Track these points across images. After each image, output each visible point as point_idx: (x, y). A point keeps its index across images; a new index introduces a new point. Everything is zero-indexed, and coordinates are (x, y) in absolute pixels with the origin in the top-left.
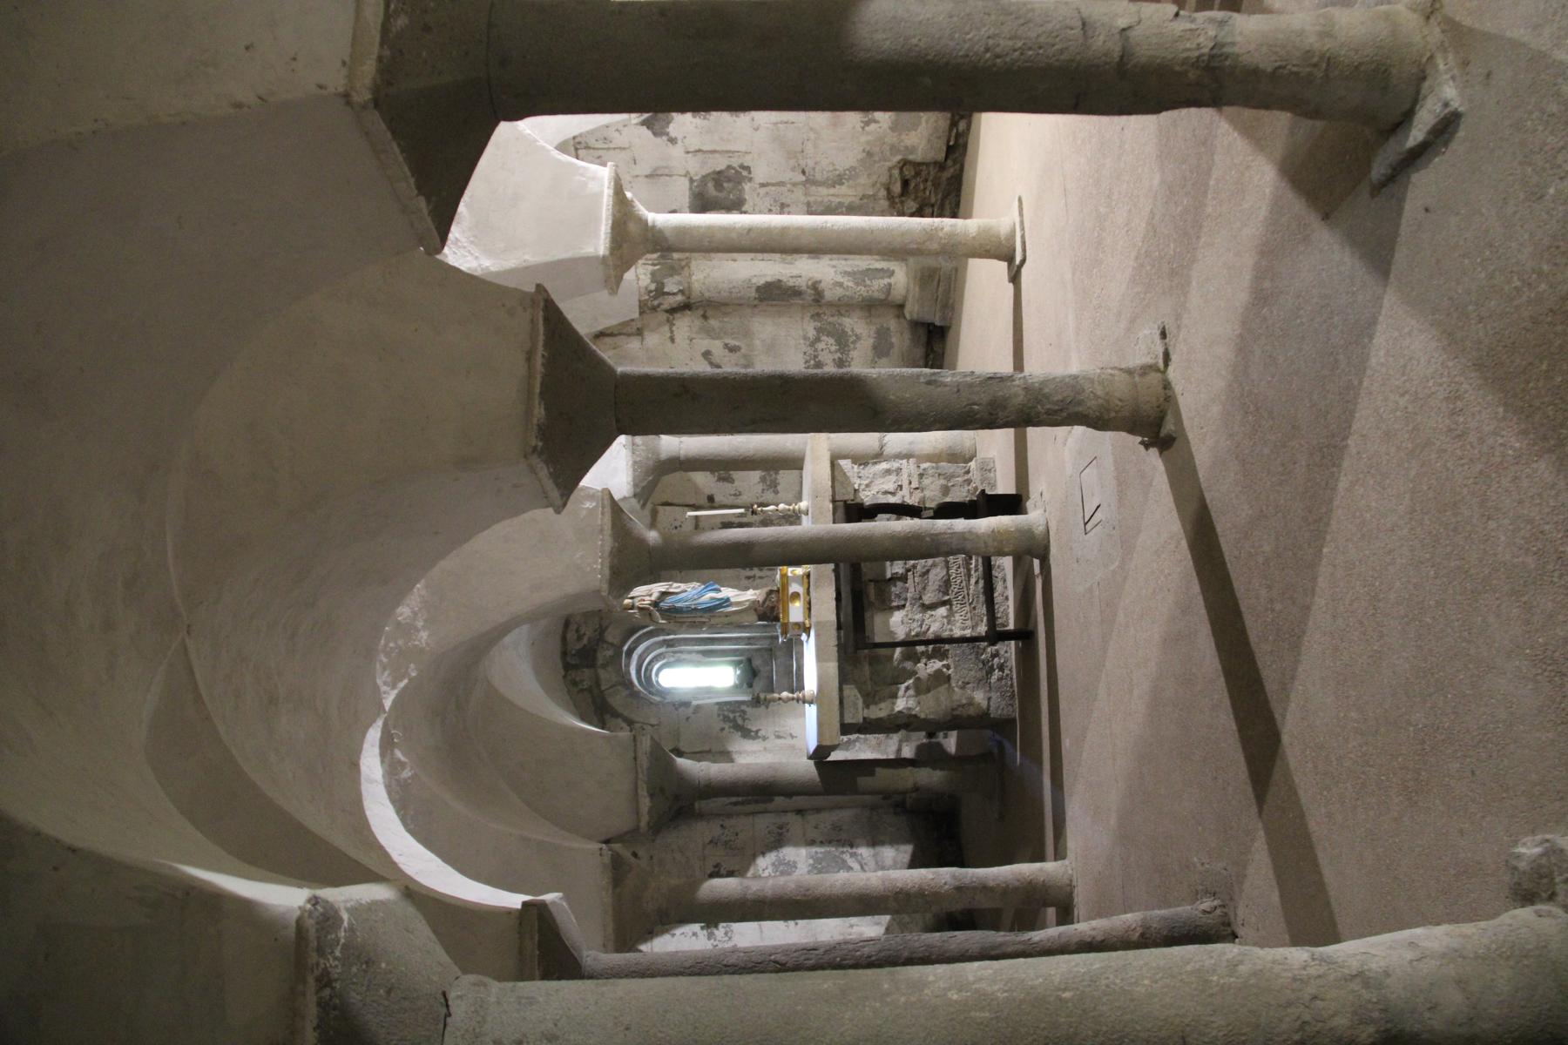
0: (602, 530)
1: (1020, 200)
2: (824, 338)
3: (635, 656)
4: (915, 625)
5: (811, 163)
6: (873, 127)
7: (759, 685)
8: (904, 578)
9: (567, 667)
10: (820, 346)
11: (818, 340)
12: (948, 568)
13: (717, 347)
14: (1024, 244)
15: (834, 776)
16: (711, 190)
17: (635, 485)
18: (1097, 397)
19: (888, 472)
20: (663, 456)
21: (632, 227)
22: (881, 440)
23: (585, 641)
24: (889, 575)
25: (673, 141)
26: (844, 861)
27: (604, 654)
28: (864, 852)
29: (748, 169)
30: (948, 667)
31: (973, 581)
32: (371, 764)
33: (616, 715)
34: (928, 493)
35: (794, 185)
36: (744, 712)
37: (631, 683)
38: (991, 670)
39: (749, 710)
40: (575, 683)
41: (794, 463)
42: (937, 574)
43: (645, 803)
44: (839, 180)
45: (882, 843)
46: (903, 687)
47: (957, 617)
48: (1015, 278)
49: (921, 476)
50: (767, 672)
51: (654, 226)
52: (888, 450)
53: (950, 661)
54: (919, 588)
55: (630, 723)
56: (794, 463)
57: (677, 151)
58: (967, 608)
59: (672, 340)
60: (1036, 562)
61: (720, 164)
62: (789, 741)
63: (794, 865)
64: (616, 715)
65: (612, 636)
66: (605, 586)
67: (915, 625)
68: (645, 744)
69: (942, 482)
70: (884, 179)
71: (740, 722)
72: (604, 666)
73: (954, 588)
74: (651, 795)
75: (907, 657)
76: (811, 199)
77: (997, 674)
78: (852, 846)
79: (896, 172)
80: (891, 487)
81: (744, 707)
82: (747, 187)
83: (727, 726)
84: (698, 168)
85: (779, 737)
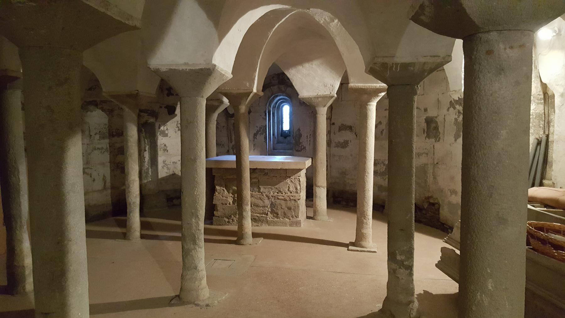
0: (238, 89)
1: (375, 252)
3: (278, 98)
5: (440, 166)
6: (449, 193)
7: (281, 139)
8: (259, 192)
10: (382, 165)
16: (433, 125)
17: (303, 99)
19: (296, 189)
20: (317, 108)
21: (365, 97)
25: (448, 110)
27: (283, 87)
29: (439, 141)
30: (229, 204)
31: (258, 215)
32: (287, 7)
35: (434, 159)
40: (273, 77)
44: (435, 178)
48: (346, 245)
49: (295, 200)
51: (367, 105)
57: (445, 111)
60: (235, 239)
61: (441, 130)
69: (292, 208)
70: (435, 197)
75: (234, 190)
76: (429, 166)
77: (227, 220)
79: (436, 201)
80: (291, 189)
82: (433, 140)
83: (258, 128)
84: (440, 120)
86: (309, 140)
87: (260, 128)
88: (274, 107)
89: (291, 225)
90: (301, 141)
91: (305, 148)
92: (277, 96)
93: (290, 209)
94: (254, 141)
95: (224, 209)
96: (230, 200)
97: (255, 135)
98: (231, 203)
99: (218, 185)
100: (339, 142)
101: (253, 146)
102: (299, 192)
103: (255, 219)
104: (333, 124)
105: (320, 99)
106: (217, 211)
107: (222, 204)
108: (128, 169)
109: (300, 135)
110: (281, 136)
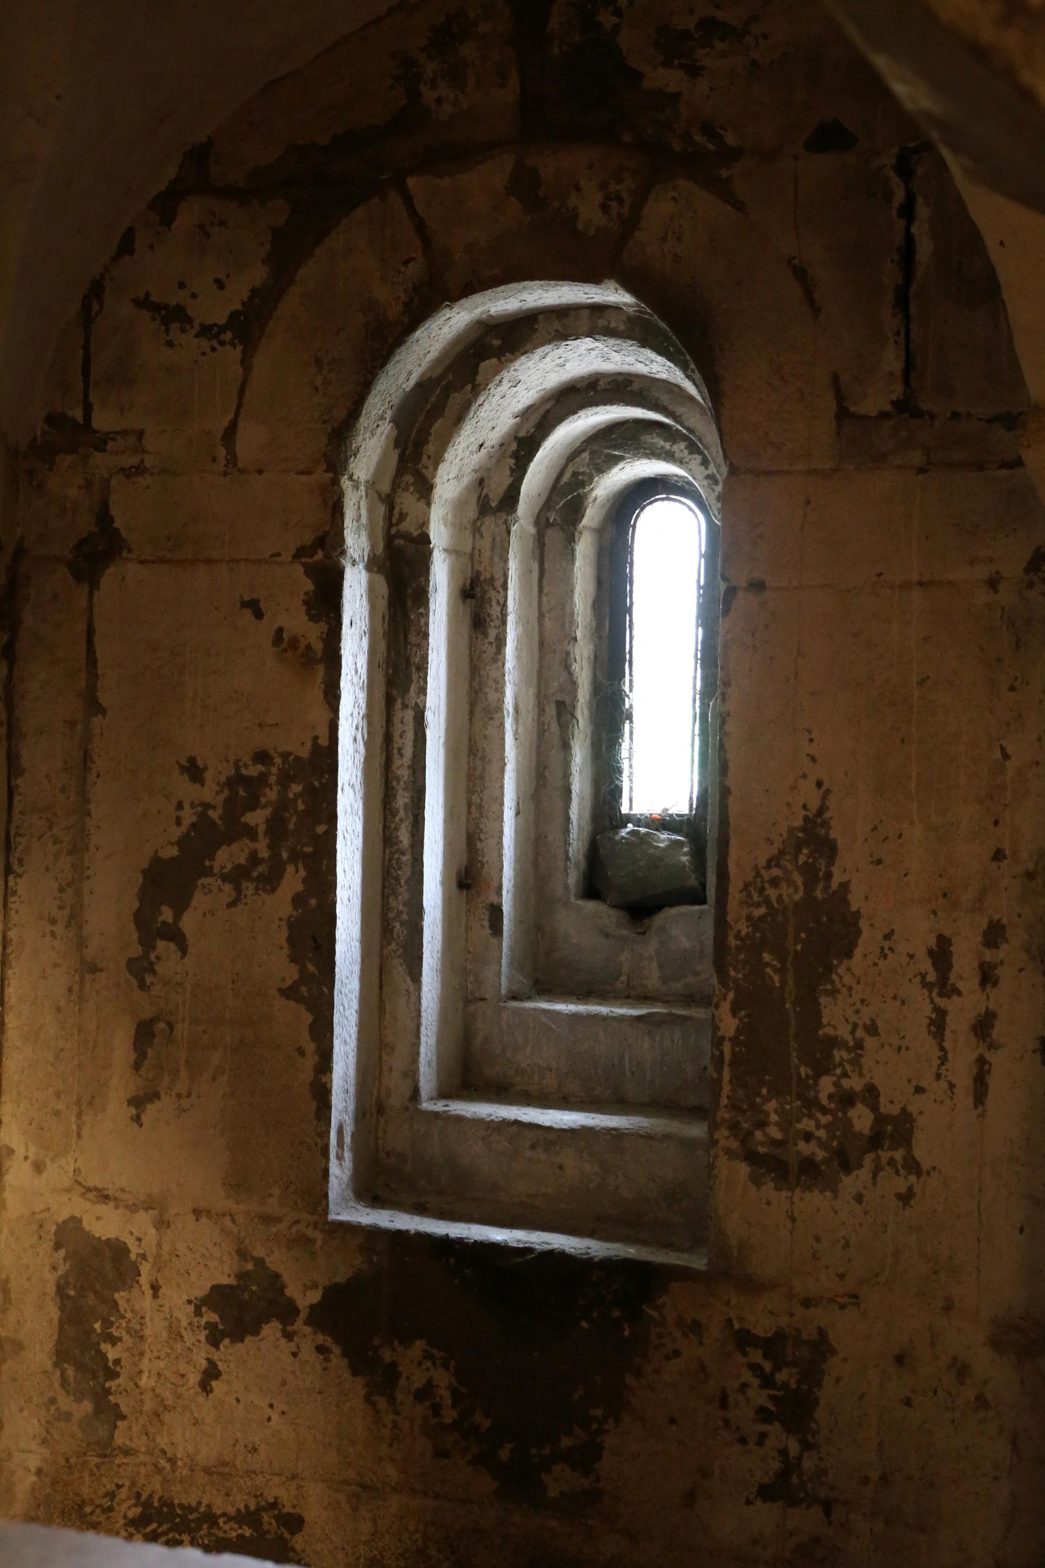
7: (585, 927)
23: (667, 78)
33: (287, 254)
36: (270, 882)
55: (246, 327)
62: (120, 1085)
64: (287, 254)
65: (676, 216)
71: (227, 857)
72: (525, 185)
81: (293, 880)
83: (209, 792)
85: (144, 1035)
86: (962, 1012)
87: (243, 790)
88: (492, 501)
90: (836, 1016)
91: (895, 1131)
92: (515, 336)
94: (141, 969)
97: (166, 885)
101: (122, 1050)
109: (829, 932)
110: (593, 887)
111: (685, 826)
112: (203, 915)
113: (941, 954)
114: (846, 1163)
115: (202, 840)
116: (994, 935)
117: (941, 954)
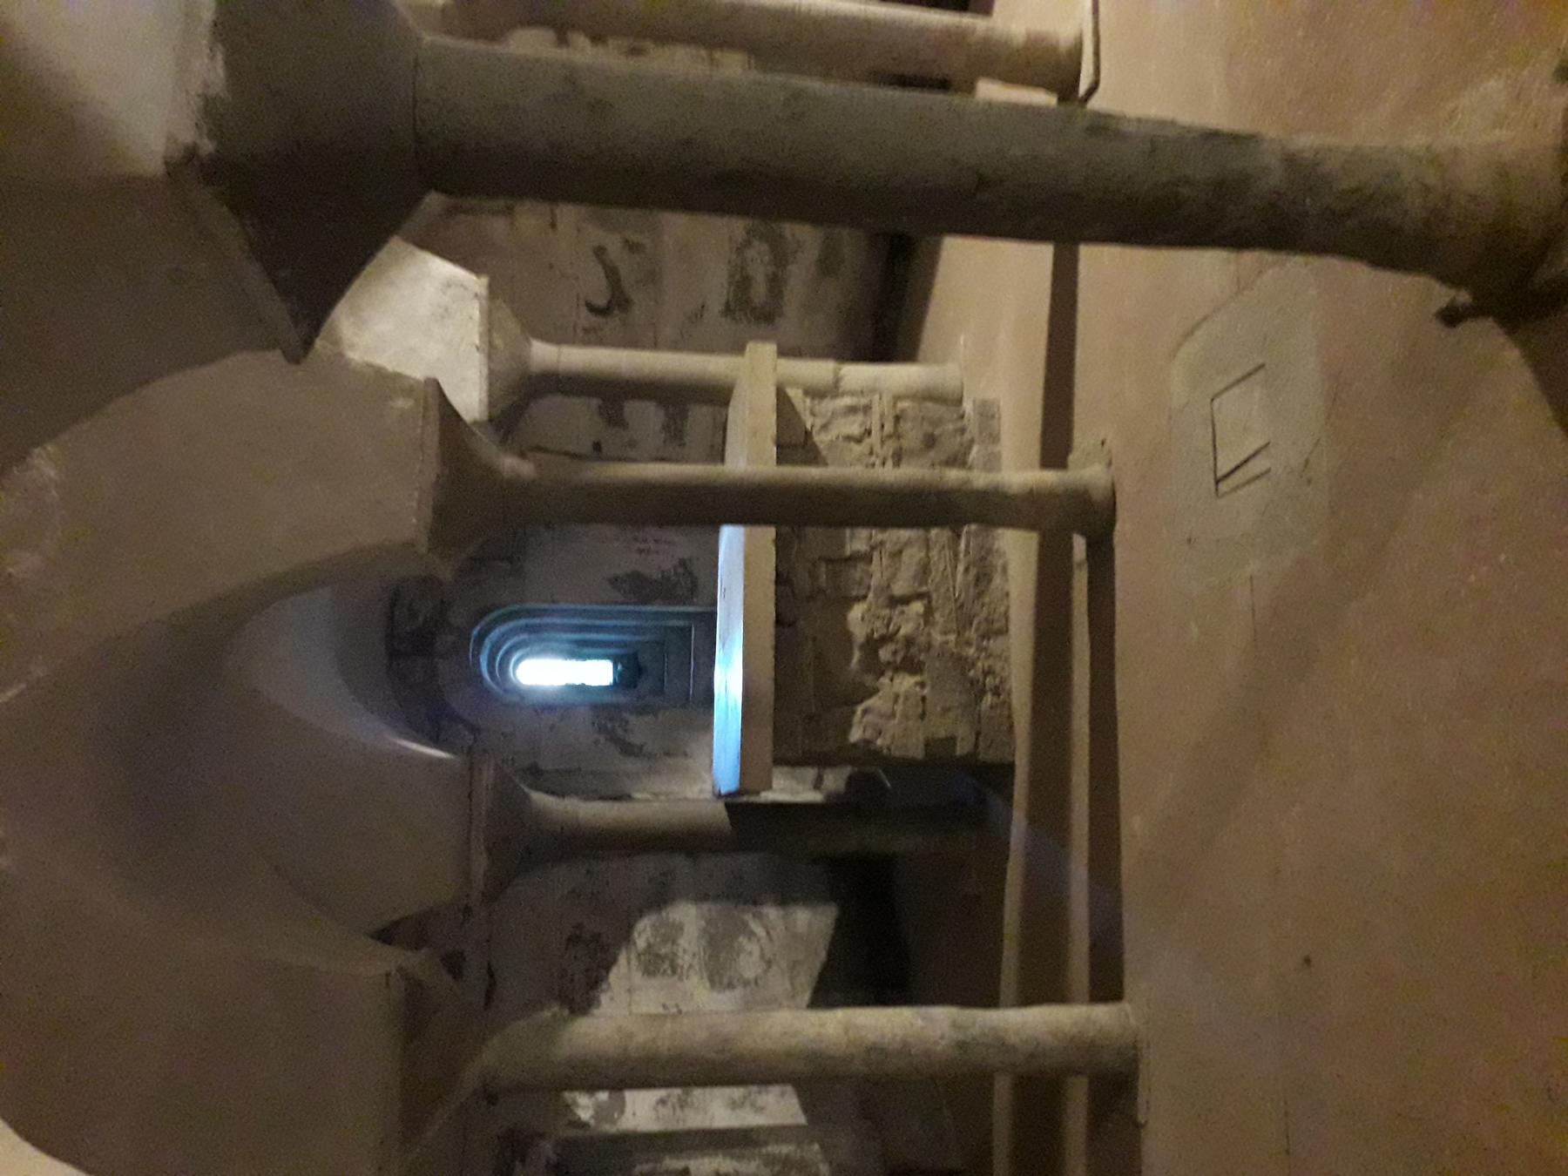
2: (756, 243)
3: (488, 643)
4: (878, 624)
7: (645, 685)
8: (866, 558)
9: (393, 654)
11: (747, 244)
12: (928, 548)
13: (614, 244)
14: (1097, 54)
15: (748, 818)
17: (491, 405)
18: (1427, 189)
19: (852, 410)
22: (836, 372)
23: (421, 619)
24: (848, 553)
26: (746, 925)
28: (772, 913)
31: (961, 568)
34: (905, 443)
37: (480, 676)
38: (983, 692)
39: (632, 719)
41: (717, 395)
42: (913, 557)
43: (480, 863)
45: (795, 901)
46: (859, 709)
47: (937, 616)
49: (897, 419)
50: (663, 675)
52: (846, 384)
53: (925, 677)
54: (887, 574)
56: (717, 395)
58: (953, 605)
59: (553, 225)
63: (680, 928)
65: (457, 618)
66: (423, 539)
67: (878, 624)
68: (487, 775)
69: (927, 428)
71: (620, 732)
73: (935, 575)
74: (490, 851)
77: (989, 699)
78: (755, 903)
80: (855, 429)
85: (668, 754)
86: (652, 545)
89: (995, 438)
90: (657, 576)
91: (683, 563)
93: (930, 442)
95: (946, 710)
96: (906, 682)
97: (628, 750)
98: (918, 678)
99: (846, 732)
100: (666, 428)
101: (670, 761)
102: (864, 401)
103: (977, 580)
104: (597, 446)
105: (498, 342)
106: (952, 739)
107: (923, 716)
108: (789, 1054)
111: (616, 660)
112: (636, 739)
113: (641, 551)
114: (691, 574)
115: (615, 739)
116: (636, 539)
117: (641, 551)
